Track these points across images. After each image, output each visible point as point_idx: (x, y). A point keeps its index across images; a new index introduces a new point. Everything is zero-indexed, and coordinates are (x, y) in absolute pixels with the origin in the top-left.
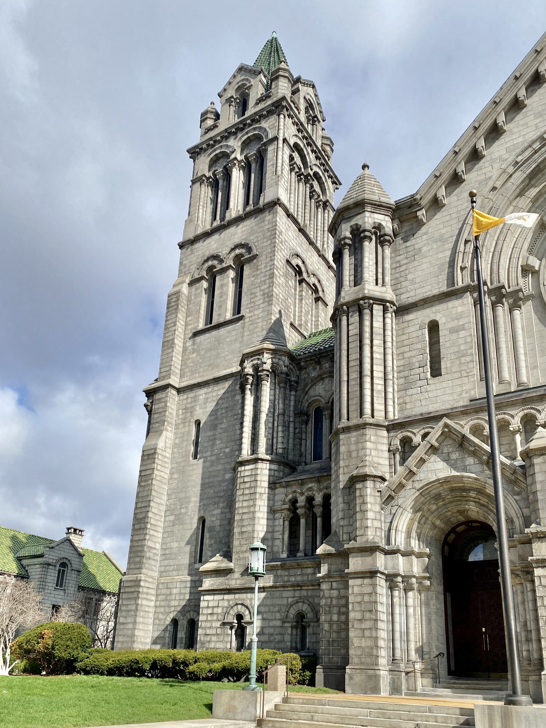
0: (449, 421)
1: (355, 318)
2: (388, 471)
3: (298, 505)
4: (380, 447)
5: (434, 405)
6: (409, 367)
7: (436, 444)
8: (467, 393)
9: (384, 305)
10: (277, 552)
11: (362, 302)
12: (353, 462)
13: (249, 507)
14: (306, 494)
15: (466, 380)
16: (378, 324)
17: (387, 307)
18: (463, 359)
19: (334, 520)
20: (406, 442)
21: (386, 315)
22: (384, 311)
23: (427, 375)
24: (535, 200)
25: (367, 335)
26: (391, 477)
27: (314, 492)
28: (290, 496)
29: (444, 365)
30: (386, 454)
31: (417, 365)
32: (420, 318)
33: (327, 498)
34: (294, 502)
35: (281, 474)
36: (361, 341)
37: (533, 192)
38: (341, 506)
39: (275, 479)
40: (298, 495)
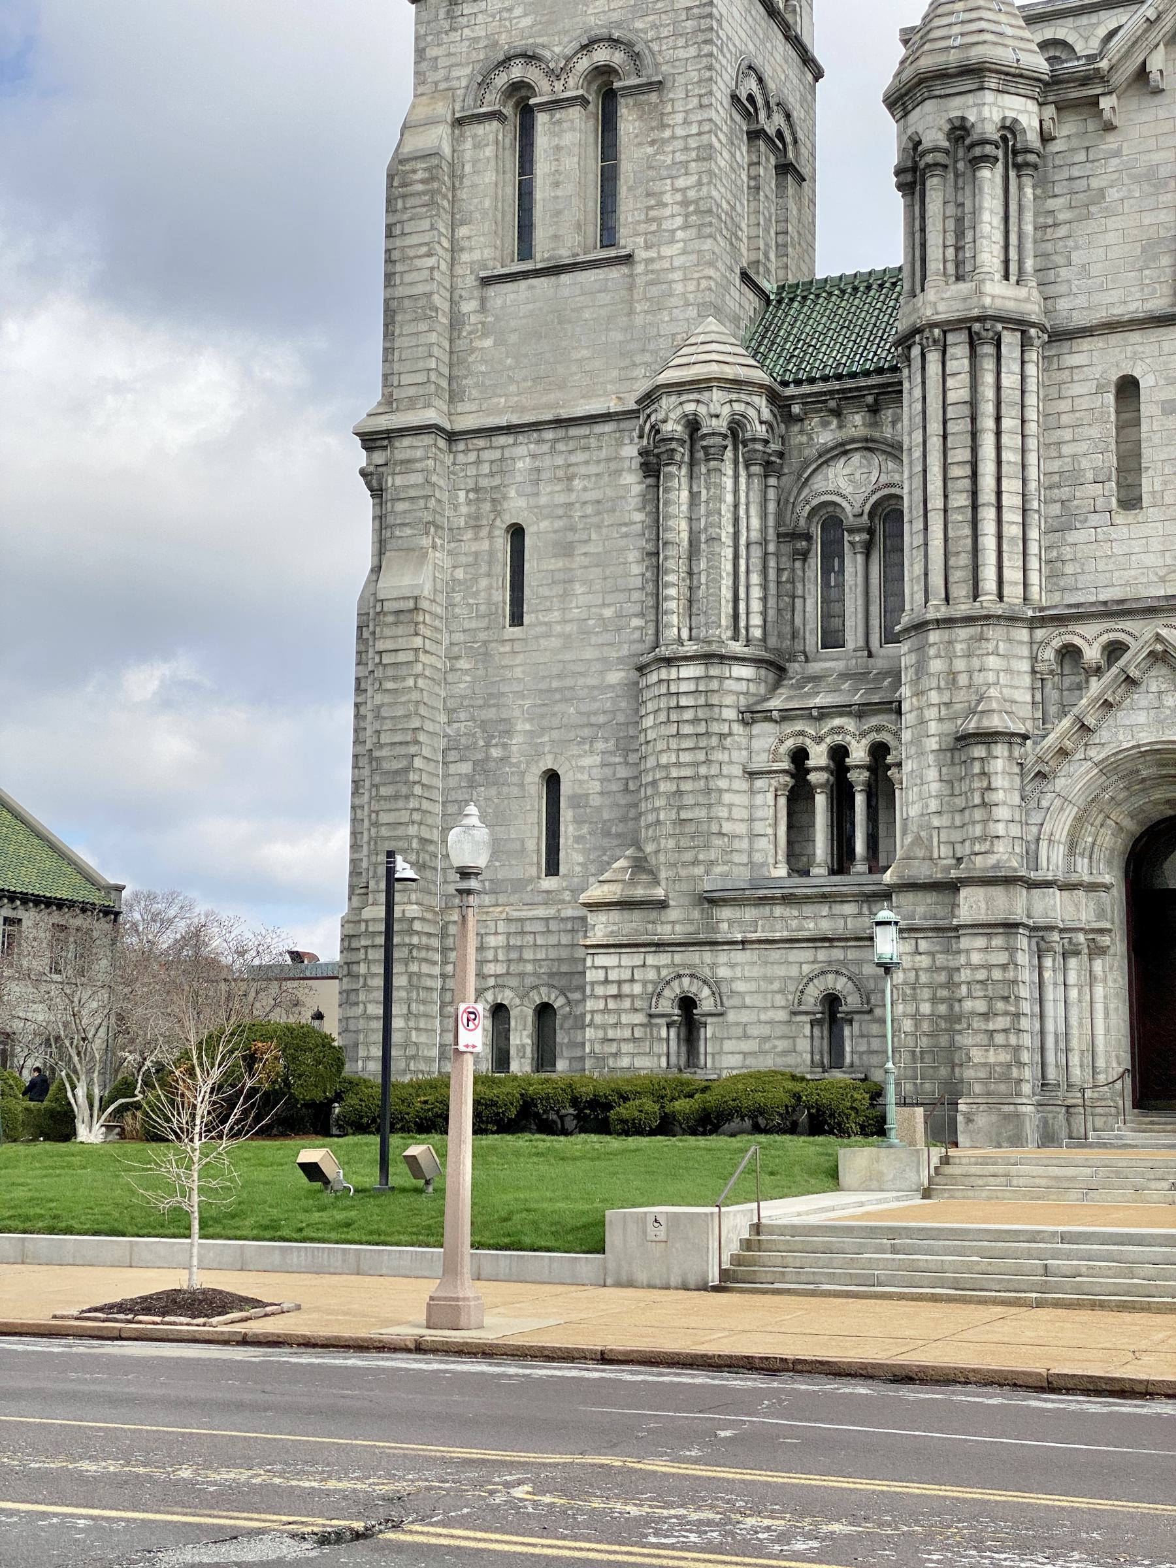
3: (811, 763)
6: (1073, 478)
9: (1023, 332)
11: (977, 327)
12: (961, 696)
13: (695, 764)
14: (828, 740)
23: (1110, 503)
27: (848, 738)
28: (790, 743)
29: (1148, 485)
30: (1027, 679)
31: (1090, 476)
34: (799, 756)
35: (762, 689)
36: (974, 419)
39: (752, 700)
40: (808, 741)
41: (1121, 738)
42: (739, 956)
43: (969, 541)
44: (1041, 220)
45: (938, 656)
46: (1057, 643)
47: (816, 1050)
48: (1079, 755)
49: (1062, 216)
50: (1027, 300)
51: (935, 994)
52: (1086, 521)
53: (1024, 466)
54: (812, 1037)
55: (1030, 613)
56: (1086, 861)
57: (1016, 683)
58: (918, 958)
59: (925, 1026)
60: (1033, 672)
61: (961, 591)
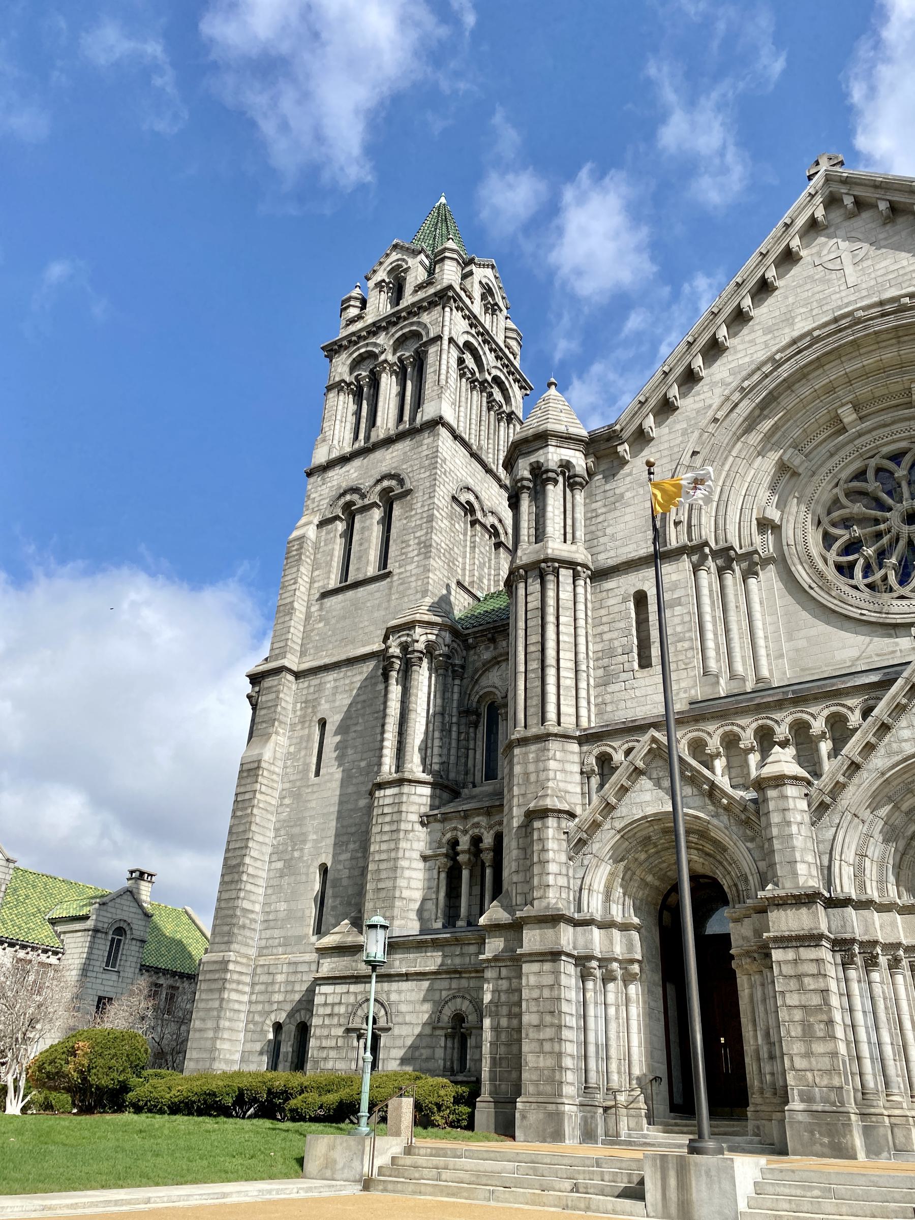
0: (657, 735)
1: (535, 586)
2: (580, 802)
3: (459, 848)
4: (568, 767)
5: (643, 708)
7: (640, 764)
8: (685, 692)
9: (574, 570)
10: (429, 920)
11: (543, 565)
12: (532, 788)
14: (470, 832)
15: (684, 674)
16: (566, 595)
17: (579, 572)
18: (679, 645)
19: (505, 873)
20: (604, 760)
21: (578, 582)
22: (574, 577)
24: (768, 436)
25: (551, 610)
26: (584, 810)
30: (578, 778)
31: (620, 650)
32: (624, 586)
33: (499, 838)
36: (543, 618)
37: (766, 425)
38: (515, 853)
41: (634, 811)
42: (405, 985)
43: (539, 689)
44: (589, 515)
45: (519, 763)
46: (596, 752)
47: (448, 1057)
48: (607, 826)
49: (600, 511)
50: (577, 552)
51: (510, 1011)
52: (619, 677)
53: (576, 645)
54: (445, 1047)
55: (578, 733)
56: (620, 907)
57: (569, 779)
58: (500, 982)
59: (503, 1037)
60: (582, 773)
61: (534, 720)
